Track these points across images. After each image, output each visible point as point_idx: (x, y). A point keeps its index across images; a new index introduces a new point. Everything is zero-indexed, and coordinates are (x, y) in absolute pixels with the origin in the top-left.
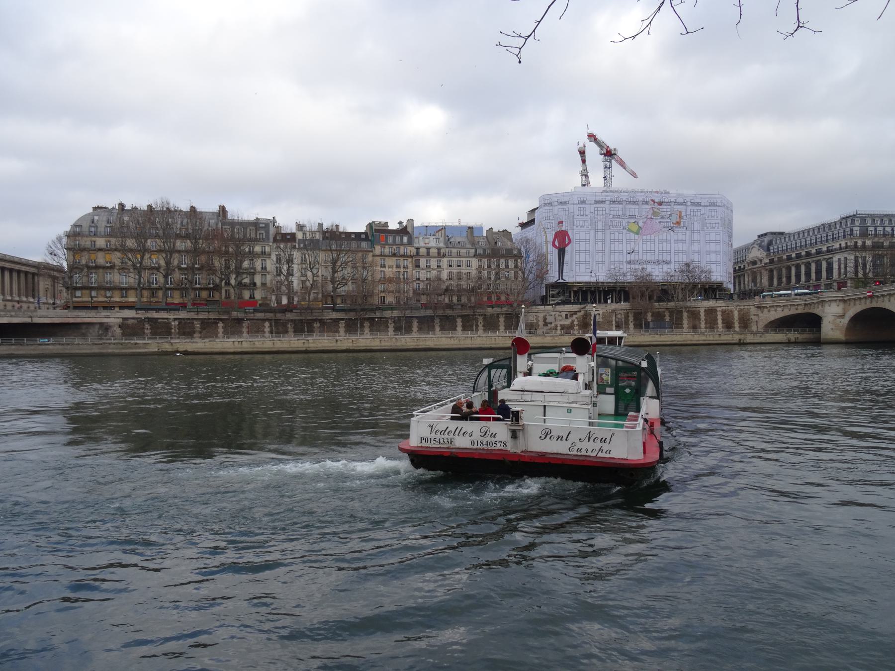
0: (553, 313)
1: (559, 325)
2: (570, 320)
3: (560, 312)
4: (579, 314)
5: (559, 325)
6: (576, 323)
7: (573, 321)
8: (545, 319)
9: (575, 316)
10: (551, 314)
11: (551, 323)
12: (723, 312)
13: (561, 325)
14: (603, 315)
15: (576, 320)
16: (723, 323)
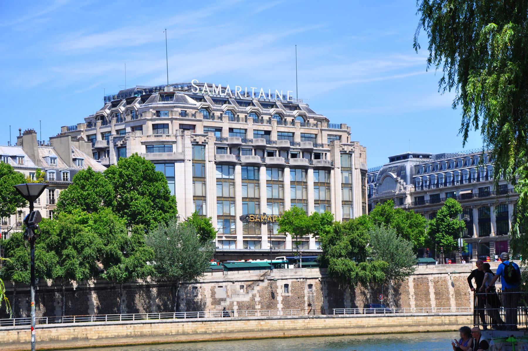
0: (224, 284)
1: (235, 303)
2: (250, 295)
3: (233, 282)
4: (261, 284)
5: (235, 303)
6: (257, 299)
7: (254, 296)
8: (213, 293)
9: (257, 288)
10: (220, 284)
11: (224, 300)
12: (436, 282)
13: (238, 303)
14: (293, 286)
15: (258, 295)
16: (436, 299)
